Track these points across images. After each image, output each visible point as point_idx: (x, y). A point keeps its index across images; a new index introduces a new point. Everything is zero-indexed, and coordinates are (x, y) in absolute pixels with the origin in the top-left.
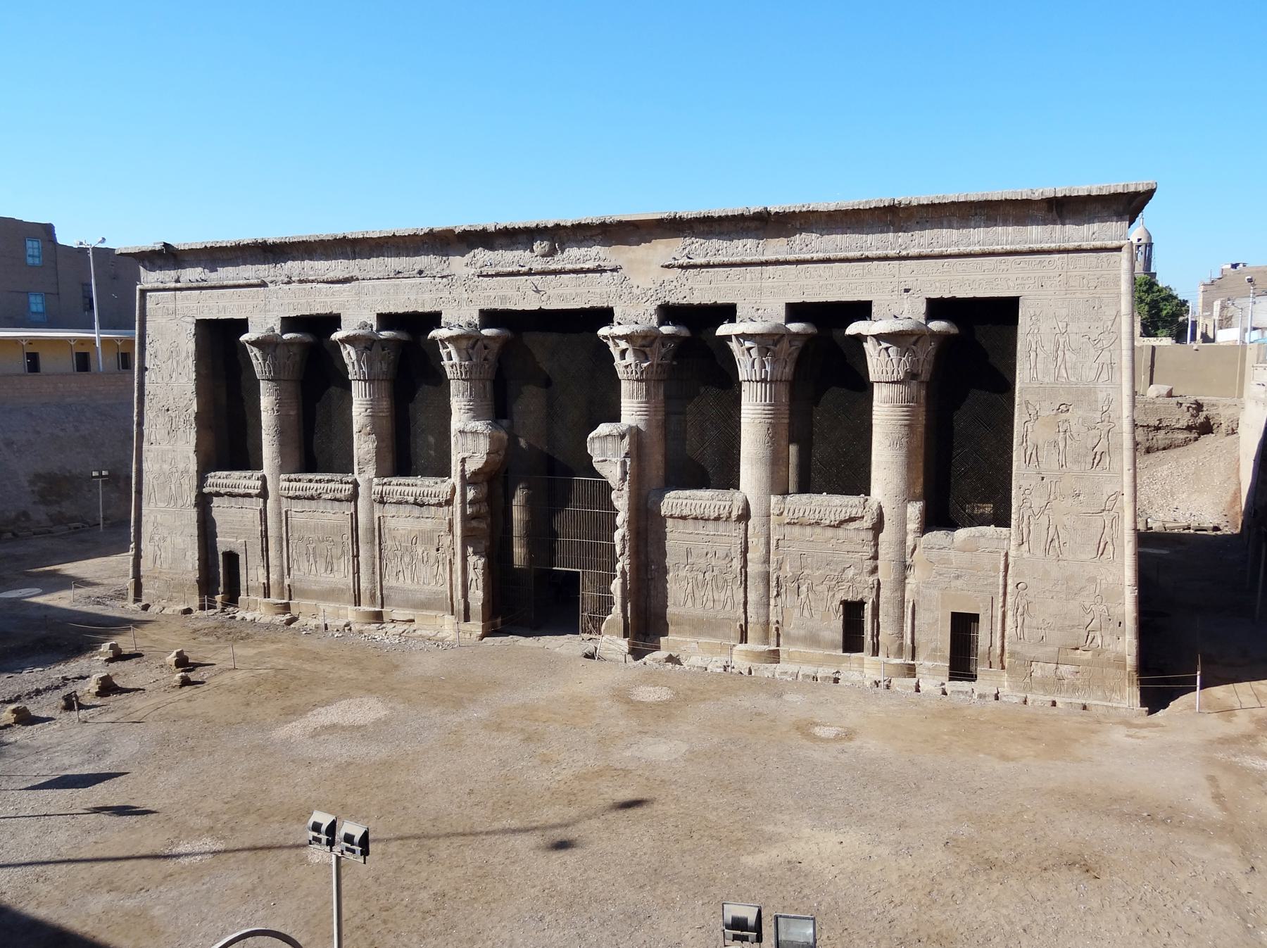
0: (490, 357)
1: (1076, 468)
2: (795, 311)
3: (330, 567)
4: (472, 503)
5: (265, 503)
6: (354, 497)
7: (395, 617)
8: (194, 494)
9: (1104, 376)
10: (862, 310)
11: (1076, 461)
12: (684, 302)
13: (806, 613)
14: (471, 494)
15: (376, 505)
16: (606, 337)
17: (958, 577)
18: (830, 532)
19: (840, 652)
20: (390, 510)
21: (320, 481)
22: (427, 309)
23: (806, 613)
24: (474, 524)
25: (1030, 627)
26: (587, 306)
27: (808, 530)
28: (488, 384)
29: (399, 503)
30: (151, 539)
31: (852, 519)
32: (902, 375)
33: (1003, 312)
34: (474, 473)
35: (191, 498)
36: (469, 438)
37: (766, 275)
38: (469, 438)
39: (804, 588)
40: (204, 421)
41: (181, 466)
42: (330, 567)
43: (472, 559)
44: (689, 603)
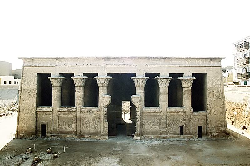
2: (170, 75)
3: (69, 126)
4: (105, 111)
5: (53, 113)
6: (76, 111)
7: (86, 136)
9: (219, 86)
10: (181, 75)
12: (150, 72)
13: (173, 129)
18: (177, 114)
21: (70, 108)
23: (173, 129)
25: (211, 127)
29: (88, 112)
30: (23, 122)
36: (104, 99)
37: (165, 68)
38: (104, 99)
41: (32, 106)
42: (69, 126)
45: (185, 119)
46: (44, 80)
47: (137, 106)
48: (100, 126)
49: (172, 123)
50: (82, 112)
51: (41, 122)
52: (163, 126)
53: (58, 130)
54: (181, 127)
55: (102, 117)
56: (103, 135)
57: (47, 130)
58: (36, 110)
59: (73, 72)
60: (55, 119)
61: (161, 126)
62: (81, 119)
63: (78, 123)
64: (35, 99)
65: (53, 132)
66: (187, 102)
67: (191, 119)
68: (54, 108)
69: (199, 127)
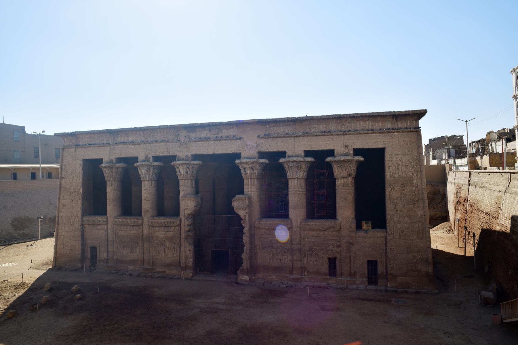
0: (194, 171)
1: (408, 207)
2: (308, 153)
5: (107, 227)
6: (142, 224)
8: (80, 224)
9: (415, 174)
10: (331, 153)
11: (408, 205)
13: (315, 263)
14: (187, 223)
15: (151, 228)
16: (238, 163)
17: (369, 247)
18: (322, 233)
19: (328, 277)
20: (156, 229)
22: (171, 154)
24: (189, 233)
26: (231, 152)
27: (315, 233)
28: (193, 181)
31: (331, 227)
32: (346, 175)
33: (380, 152)
34: (189, 214)
35: (78, 226)
37: (296, 141)
39: (314, 254)
40: (86, 197)
41: (75, 214)
43: (188, 247)
44: (271, 261)
45: (339, 244)
46: (93, 170)
47: (242, 217)
48: (180, 252)
49: (313, 252)
50: (152, 226)
51: (91, 242)
52: (295, 257)
53: (115, 257)
54: (332, 262)
55: (183, 236)
56: (185, 268)
57: (98, 256)
58: (82, 221)
59: (136, 155)
60: (110, 239)
61: (290, 258)
62: (150, 239)
63: (146, 245)
64: (80, 202)
65: (107, 260)
66: (345, 210)
67: (352, 244)
68: (109, 218)
69: (369, 262)
